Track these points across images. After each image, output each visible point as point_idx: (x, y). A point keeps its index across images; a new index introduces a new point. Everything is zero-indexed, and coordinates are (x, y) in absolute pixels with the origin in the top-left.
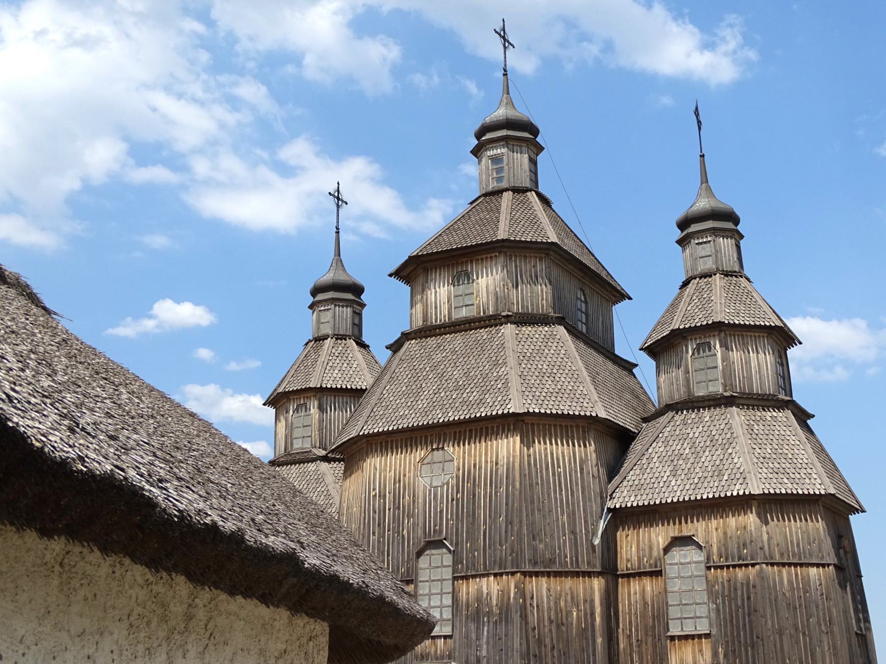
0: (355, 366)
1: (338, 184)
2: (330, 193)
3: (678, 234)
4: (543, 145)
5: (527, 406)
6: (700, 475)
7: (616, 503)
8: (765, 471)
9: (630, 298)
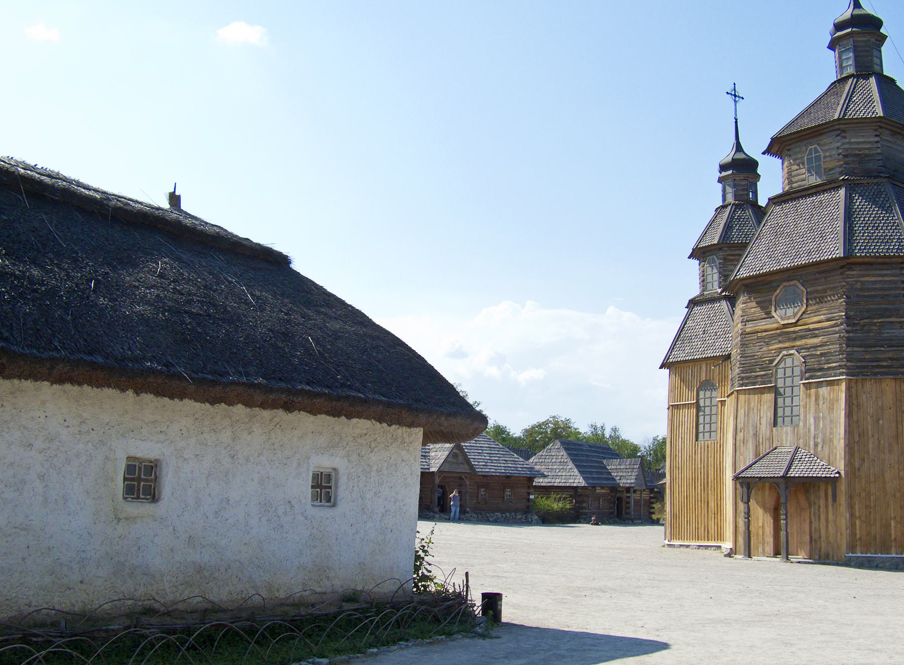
1: (734, 84)
2: (727, 93)
4: (887, 35)
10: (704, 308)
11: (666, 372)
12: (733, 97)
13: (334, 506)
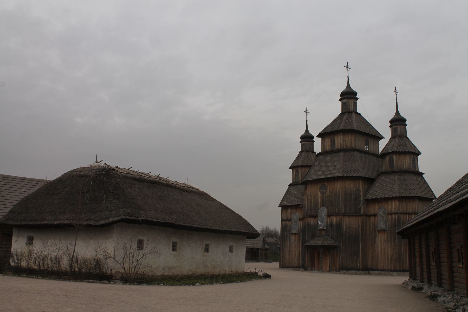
0: (310, 159)
2: (304, 111)
3: (390, 124)
4: (358, 98)
5: (343, 174)
6: (386, 191)
7: (367, 198)
8: (402, 190)
9: (385, 138)
10: (295, 187)
11: (281, 208)
12: (306, 113)
13: (232, 253)
